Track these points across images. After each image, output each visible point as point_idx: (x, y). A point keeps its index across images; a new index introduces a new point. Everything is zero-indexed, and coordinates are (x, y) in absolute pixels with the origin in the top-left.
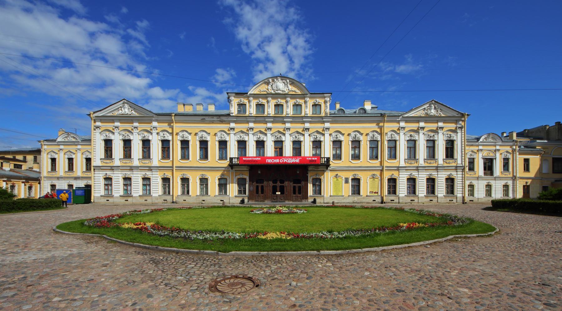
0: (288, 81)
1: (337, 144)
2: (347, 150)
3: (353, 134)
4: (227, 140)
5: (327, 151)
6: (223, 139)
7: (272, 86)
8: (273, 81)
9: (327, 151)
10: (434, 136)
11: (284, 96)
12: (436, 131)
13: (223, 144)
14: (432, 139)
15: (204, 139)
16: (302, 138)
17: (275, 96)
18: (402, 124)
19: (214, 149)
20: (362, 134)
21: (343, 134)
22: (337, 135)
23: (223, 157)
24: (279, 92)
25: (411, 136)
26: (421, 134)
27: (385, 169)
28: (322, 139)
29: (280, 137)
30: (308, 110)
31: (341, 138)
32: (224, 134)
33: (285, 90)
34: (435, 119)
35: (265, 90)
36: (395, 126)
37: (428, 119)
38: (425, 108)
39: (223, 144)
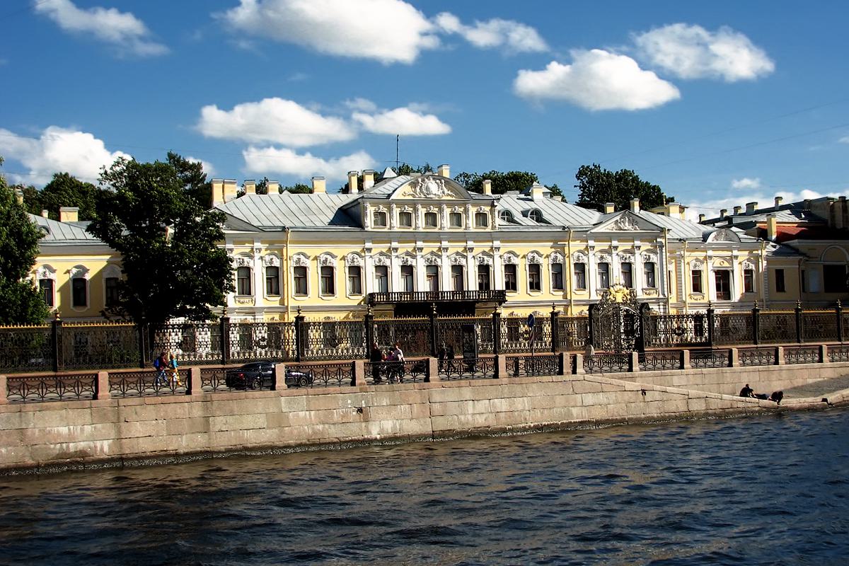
0: (443, 181)
1: (511, 269)
2: (523, 277)
3: (530, 256)
4: (361, 265)
5: (499, 283)
6: (356, 264)
7: (421, 187)
8: (423, 181)
9: (499, 283)
10: (629, 257)
11: (439, 204)
12: (631, 252)
13: (355, 272)
14: (627, 261)
15: (328, 264)
16: (463, 262)
17: (427, 202)
18: (591, 243)
19: (342, 280)
20: (541, 256)
21: (517, 256)
22: (510, 257)
23: (357, 289)
24: (431, 196)
25: (602, 258)
26: (614, 255)
27: (573, 303)
28: (490, 263)
29: (436, 260)
30: (471, 223)
31: (515, 261)
32: (358, 256)
33: (439, 193)
34: (631, 237)
35: (412, 193)
36: (582, 246)
37: (623, 237)
38: (617, 221)
39: (355, 272)
